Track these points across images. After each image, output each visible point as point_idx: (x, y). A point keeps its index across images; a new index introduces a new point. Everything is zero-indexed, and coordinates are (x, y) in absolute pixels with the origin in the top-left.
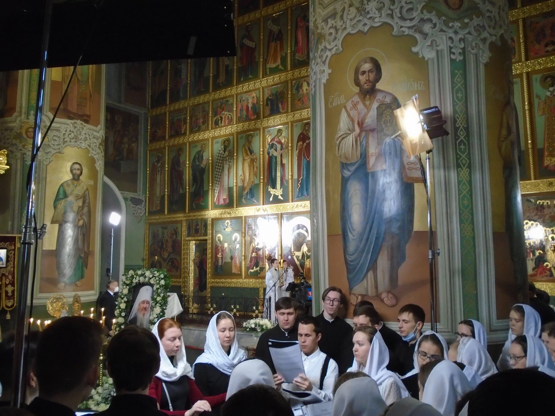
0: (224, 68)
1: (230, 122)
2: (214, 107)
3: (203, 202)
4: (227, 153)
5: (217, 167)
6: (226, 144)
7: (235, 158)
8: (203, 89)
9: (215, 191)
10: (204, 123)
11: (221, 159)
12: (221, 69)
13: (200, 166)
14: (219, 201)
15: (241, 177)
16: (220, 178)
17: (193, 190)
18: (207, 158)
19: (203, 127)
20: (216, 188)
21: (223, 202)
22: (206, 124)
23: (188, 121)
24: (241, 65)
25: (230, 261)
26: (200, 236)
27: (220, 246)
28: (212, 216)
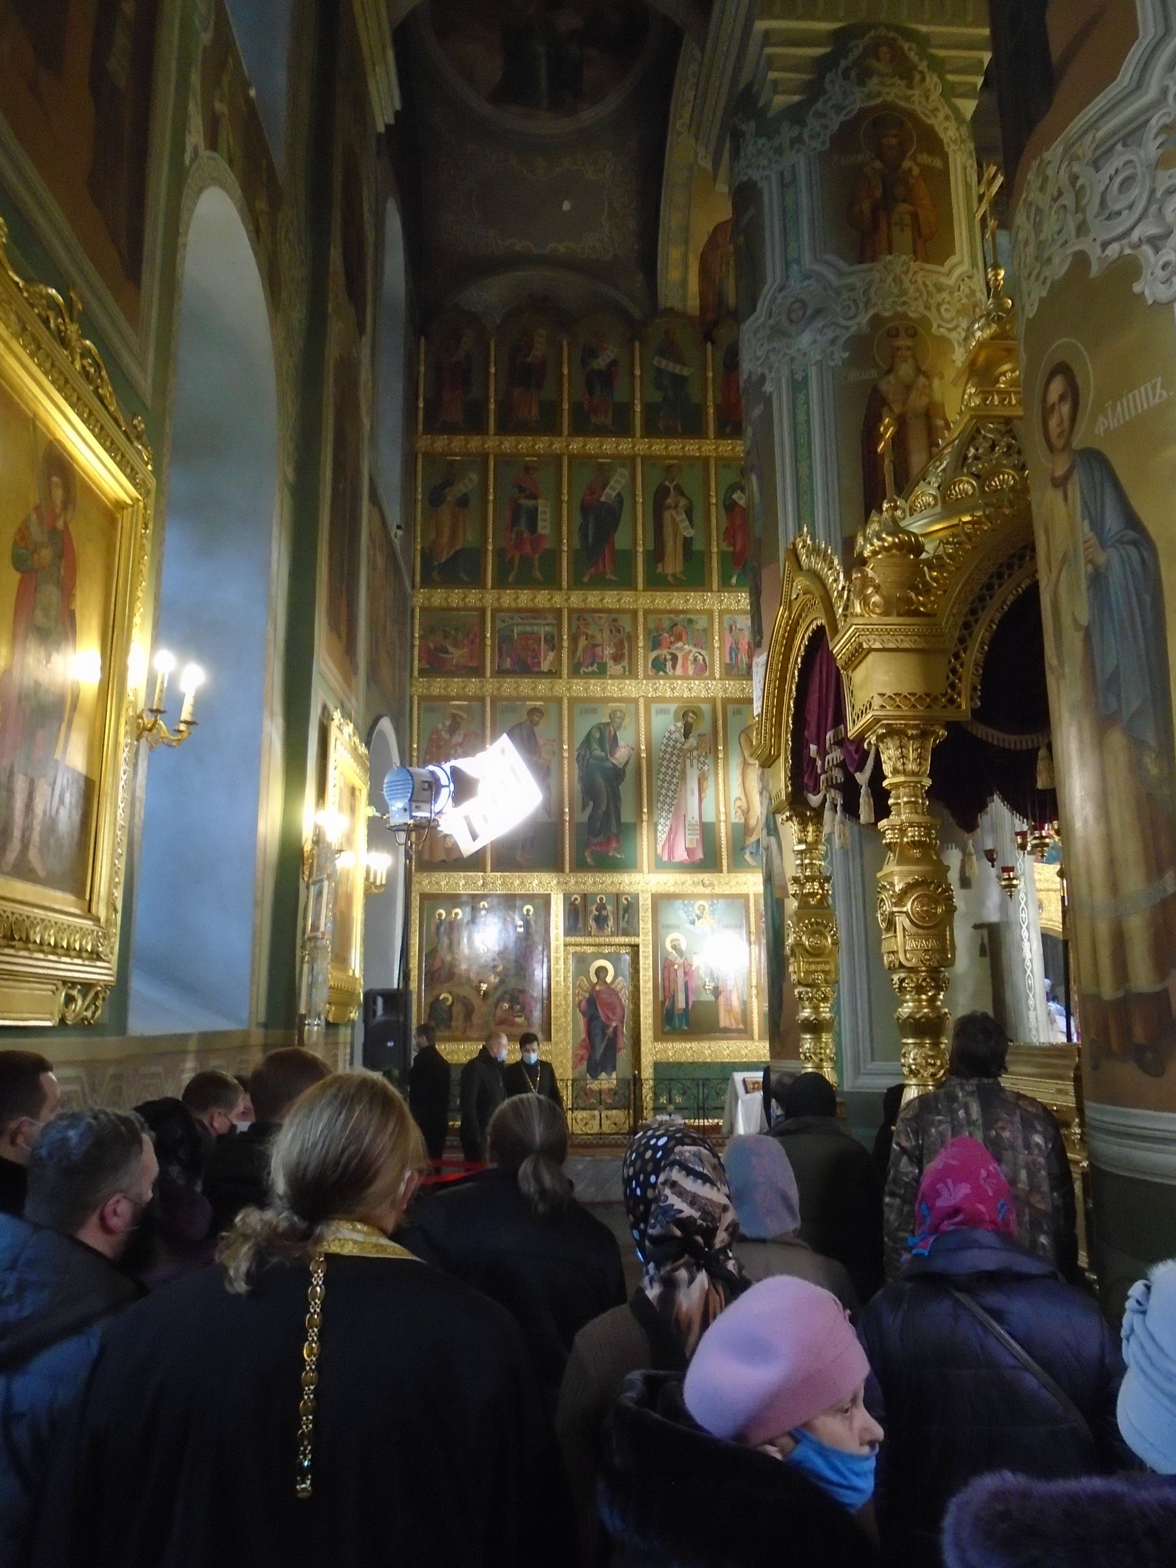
0: (680, 543)
1: (702, 670)
2: (651, 625)
3: (618, 850)
4: (692, 741)
5: (663, 770)
6: (689, 717)
7: (721, 756)
8: (609, 576)
9: (660, 828)
10: (617, 658)
11: (676, 752)
12: (670, 544)
13: (607, 760)
14: (671, 853)
15: (738, 803)
16: (673, 798)
17: (584, 818)
18: (632, 743)
19: (614, 668)
20: (662, 821)
21: (686, 857)
22: (625, 663)
23: (565, 644)
24: (731, 549)
25: (711, 998)
26: (612, 935)
27: (679, 961)
28: (655, 889)
